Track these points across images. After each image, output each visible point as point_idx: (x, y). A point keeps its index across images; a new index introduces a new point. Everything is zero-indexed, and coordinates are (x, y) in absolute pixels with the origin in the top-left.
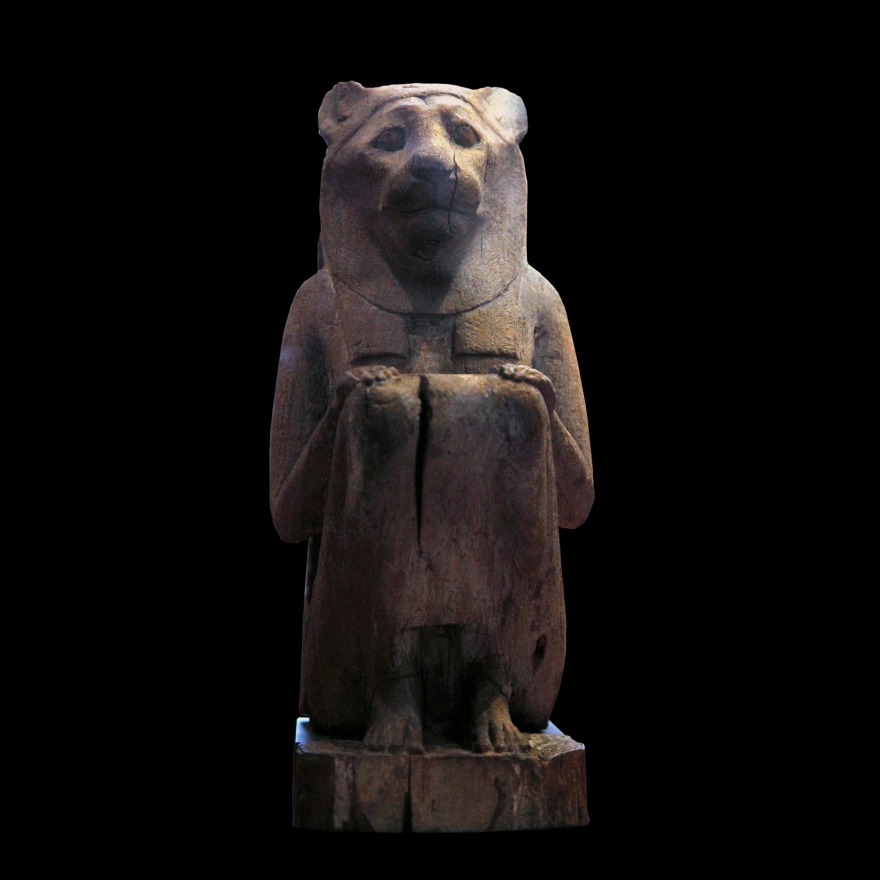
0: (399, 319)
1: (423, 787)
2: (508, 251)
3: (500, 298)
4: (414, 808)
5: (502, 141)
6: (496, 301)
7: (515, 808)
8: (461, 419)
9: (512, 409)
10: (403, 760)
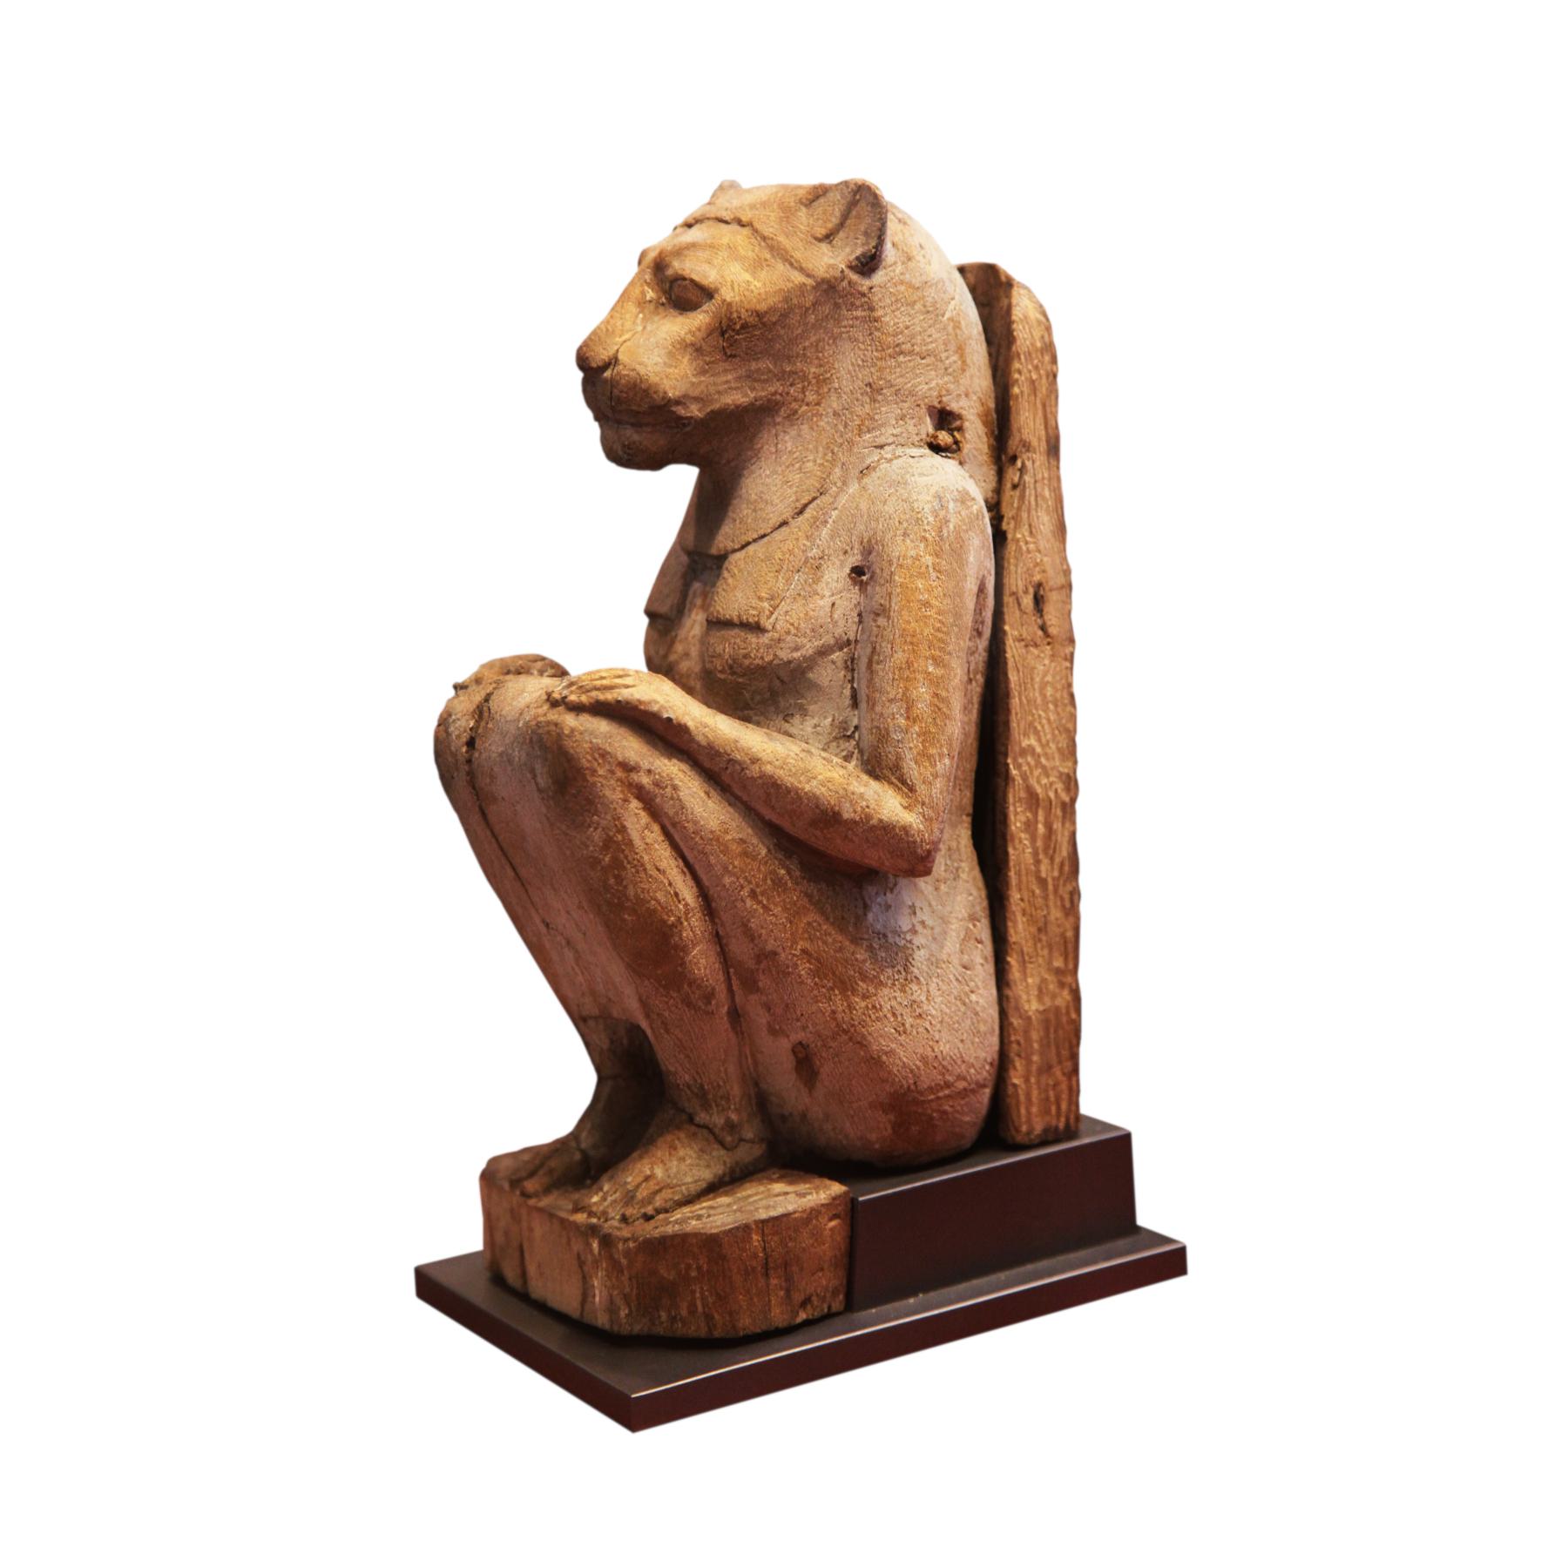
5: (799, 278)
6: (775, 534)
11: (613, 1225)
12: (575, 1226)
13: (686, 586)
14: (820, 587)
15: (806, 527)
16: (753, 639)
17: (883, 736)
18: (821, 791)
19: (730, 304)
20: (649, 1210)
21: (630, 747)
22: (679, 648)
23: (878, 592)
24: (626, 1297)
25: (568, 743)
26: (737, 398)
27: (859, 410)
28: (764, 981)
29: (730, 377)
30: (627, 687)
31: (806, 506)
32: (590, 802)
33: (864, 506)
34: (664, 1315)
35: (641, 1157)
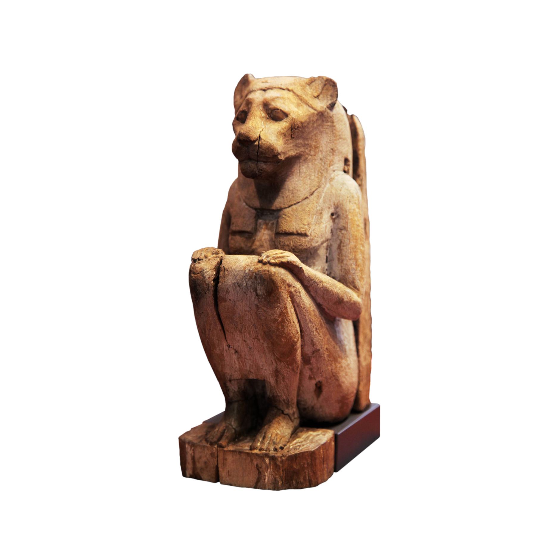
0: (254, 211)
1: (223, 463)
2: (319, 171)
3: (306, 200)
4: (220, 473)
5: (312, 111)
6: (303, 202)
7: (266, 480)
8: (234, 283)
9: (259, 280)
10: (214, 449)
11: (272, 453)
12: (257, 454)
13: (256, 221)
14: (323, 220)
15: (315, 199)
16: (303, 239)
17: (347, 272)
18: (339, 291)
19: (295, 119)
20: (281, 445)
21: (289, 278)
22: (257, 243)
23: (342, 223)
24: (281, 478)
25: (274, 278)
26: (292, 153)
27: (329, 158)
28: (313, 360)
29: (291, 145)
30: (287, 257)
31: (314, 192)
32: (278, 298)
33: (334, 191)
34: (294, 482)
35: (269, 428)
